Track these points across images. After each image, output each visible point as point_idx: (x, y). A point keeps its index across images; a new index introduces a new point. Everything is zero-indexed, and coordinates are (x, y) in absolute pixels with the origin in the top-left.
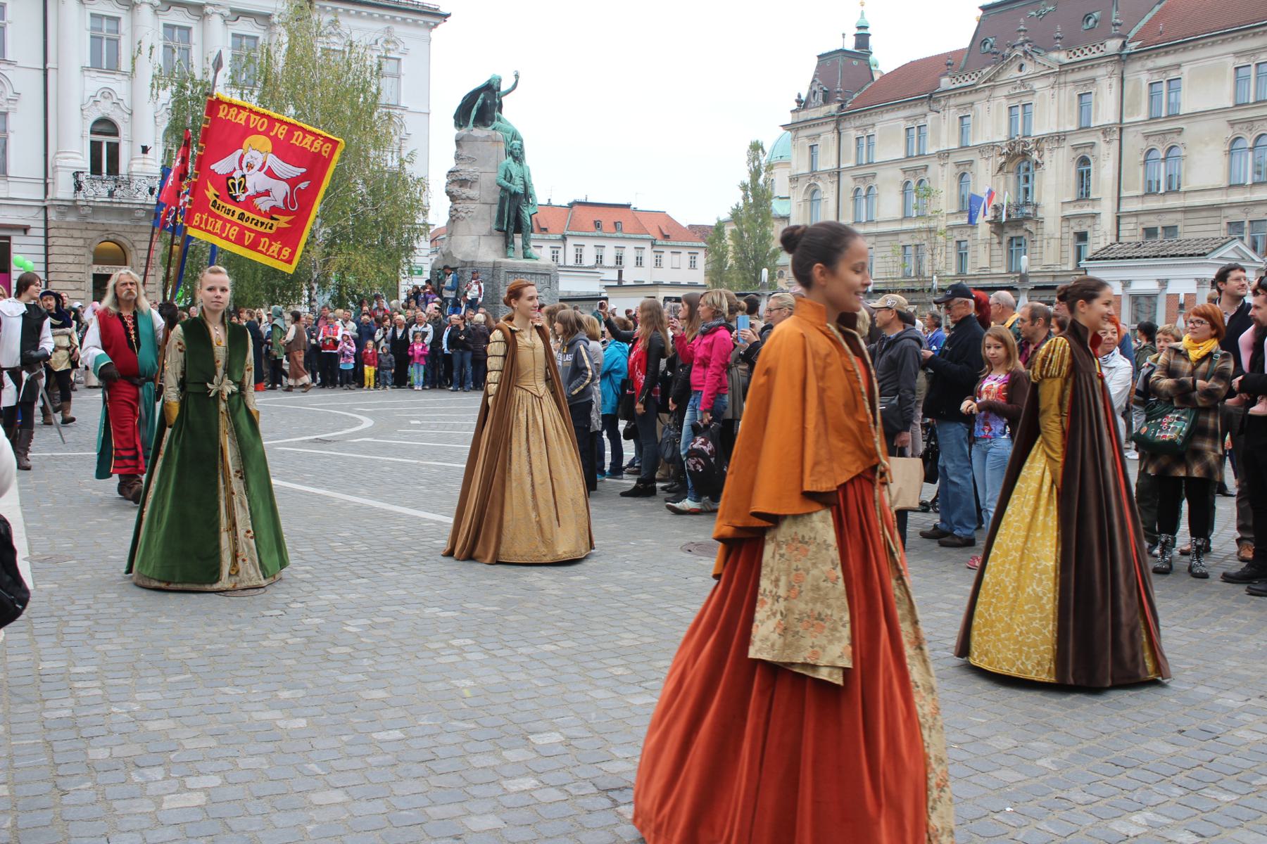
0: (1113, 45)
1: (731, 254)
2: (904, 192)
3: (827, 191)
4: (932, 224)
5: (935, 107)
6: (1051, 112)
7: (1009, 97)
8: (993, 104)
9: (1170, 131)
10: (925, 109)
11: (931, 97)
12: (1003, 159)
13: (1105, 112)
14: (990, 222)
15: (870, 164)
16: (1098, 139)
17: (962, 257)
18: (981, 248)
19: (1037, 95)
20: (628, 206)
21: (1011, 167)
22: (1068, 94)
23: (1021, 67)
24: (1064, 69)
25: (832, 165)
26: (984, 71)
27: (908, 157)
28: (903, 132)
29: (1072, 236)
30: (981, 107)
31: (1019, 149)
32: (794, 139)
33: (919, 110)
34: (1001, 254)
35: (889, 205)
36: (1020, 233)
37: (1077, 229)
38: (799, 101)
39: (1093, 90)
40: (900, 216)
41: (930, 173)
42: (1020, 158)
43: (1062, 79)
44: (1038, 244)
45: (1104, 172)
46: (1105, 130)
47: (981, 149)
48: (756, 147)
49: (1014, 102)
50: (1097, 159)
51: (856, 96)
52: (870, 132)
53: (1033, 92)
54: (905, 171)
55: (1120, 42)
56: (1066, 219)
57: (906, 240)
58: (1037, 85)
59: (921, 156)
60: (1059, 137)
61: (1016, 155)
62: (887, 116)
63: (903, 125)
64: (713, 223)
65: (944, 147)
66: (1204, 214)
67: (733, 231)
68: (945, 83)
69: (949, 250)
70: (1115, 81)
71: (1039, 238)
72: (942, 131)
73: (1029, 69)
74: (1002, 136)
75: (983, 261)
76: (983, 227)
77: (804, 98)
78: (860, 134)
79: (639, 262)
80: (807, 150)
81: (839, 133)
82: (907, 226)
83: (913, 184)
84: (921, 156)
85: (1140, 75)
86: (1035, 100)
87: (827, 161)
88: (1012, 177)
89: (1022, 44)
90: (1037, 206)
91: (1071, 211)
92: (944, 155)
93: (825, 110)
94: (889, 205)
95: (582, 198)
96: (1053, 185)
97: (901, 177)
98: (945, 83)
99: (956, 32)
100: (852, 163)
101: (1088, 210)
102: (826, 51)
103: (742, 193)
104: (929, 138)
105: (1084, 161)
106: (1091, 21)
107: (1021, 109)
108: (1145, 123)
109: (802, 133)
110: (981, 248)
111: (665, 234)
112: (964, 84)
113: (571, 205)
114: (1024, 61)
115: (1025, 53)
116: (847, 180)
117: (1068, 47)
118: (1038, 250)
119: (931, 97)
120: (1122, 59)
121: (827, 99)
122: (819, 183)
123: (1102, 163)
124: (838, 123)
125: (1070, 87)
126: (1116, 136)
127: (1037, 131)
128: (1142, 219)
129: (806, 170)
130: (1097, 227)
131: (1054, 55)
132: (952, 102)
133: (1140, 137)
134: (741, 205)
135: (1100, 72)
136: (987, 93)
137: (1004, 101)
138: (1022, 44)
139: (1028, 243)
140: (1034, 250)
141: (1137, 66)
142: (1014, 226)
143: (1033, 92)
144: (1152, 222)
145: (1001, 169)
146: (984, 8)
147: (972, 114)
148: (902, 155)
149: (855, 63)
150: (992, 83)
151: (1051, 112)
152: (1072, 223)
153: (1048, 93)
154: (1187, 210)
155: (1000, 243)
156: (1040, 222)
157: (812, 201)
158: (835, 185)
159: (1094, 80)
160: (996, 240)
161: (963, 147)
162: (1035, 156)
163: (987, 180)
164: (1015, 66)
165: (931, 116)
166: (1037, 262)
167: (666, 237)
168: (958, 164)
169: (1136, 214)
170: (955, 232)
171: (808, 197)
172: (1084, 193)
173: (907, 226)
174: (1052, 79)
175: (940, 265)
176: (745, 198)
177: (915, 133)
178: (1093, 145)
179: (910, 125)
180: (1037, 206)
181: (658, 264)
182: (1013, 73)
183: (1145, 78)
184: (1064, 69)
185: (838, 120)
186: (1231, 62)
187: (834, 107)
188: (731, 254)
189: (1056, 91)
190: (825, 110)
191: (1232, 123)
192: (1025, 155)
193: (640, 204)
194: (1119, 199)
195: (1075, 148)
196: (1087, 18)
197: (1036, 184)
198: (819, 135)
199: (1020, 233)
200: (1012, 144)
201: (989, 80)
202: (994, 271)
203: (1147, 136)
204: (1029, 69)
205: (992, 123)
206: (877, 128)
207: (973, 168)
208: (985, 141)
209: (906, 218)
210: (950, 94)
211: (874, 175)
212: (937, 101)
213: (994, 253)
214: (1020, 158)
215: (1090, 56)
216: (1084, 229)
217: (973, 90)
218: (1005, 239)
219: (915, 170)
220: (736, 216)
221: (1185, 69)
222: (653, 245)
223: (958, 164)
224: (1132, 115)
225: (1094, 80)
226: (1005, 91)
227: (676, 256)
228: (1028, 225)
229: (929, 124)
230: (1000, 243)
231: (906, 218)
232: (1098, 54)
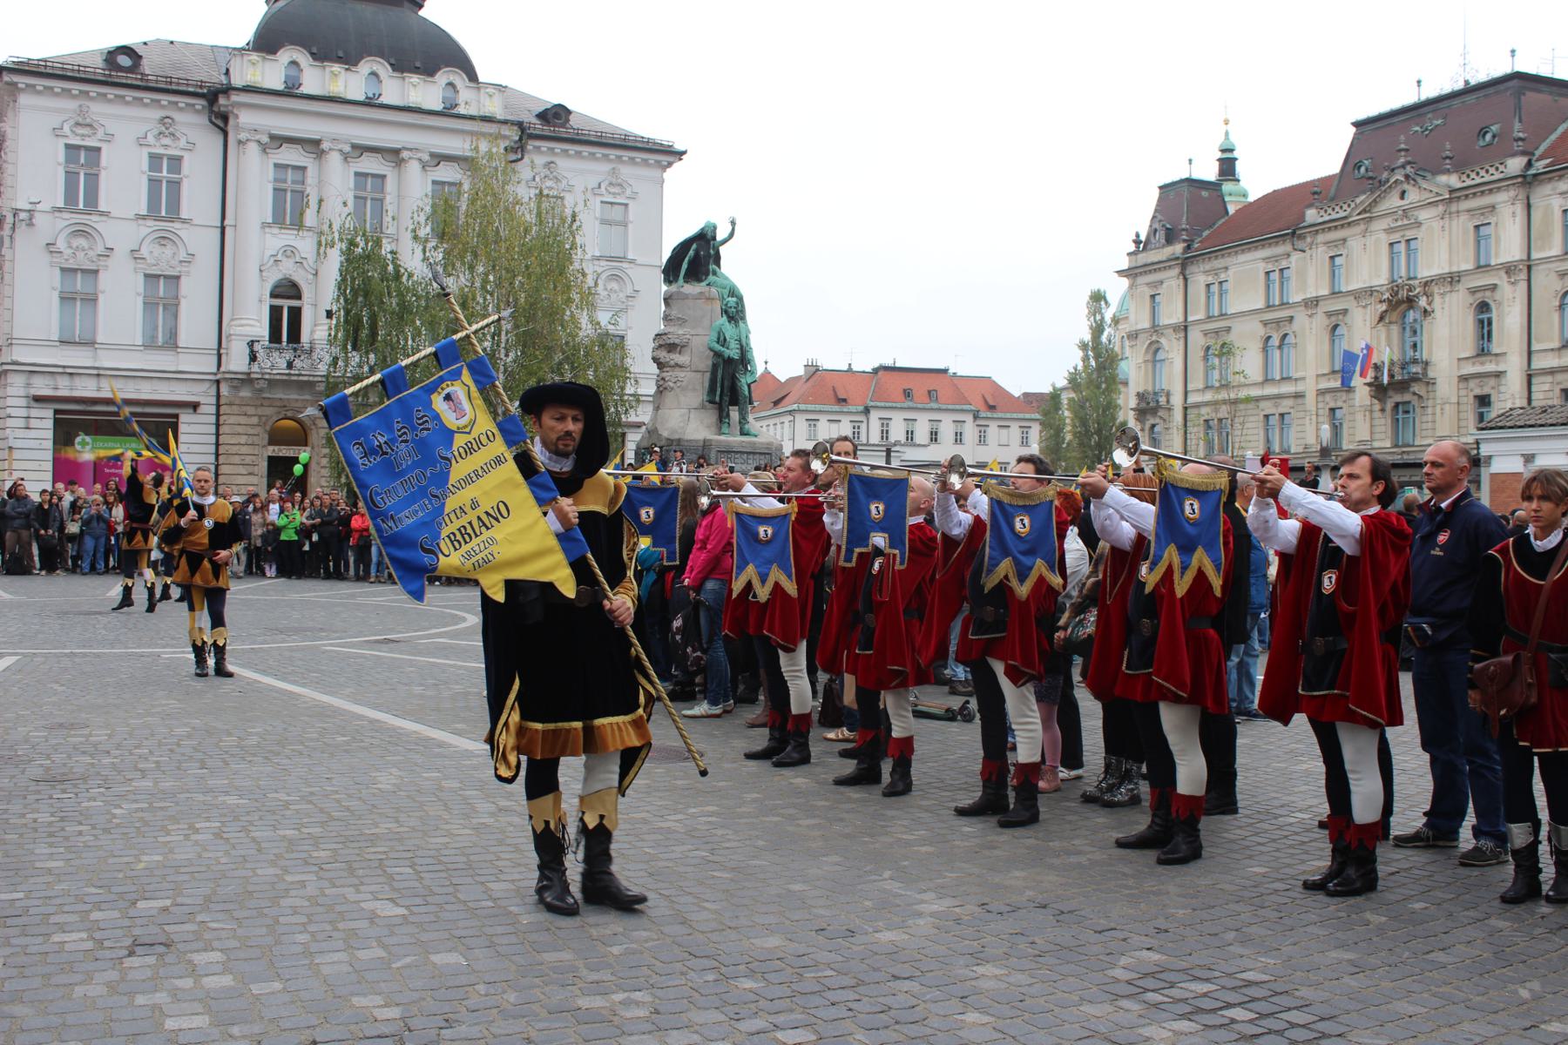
0: (1515, 165)
1: (1068, 428)
2: (1265, 350)
3: (1172, 350)
4: (1300, 387)
5: (1300, 244)
6: (1441, 248)
7: (1389, 231)
8: (1370, 240)
10: (1287, 247)
12: (1384, 307)
13: (1509, 246)
14: (1369, 384)
16: (1501, 279)
17: (1336, 429)
18: (1359, 416)
19: (1423, 228)
20: (945, 371)
21: (1395, 316)
23: (1403, 195)
24: (1455, 195)
25: (1177, 318)
26: (1358, 200)
28: (1262, 276)
29: (1471, 400)
30: (1355, 244)
31: (1403, 294)
32: (1131, 287)
34: (1384, 423)
35: (1249, 363)
36: (1407, 397)
37: (1478, 392)
38: (1137, 242)
40: (1260, 379)
41: (1296, 325)
42: (1402, 303)
43: (1454, 207)
44: (1430, 411)
45: (1509, 320)
46: (1509, 269)
47: (1357, 295)
48: (1098, 298)
49: (1395, 237)
50: (1500, 304)
51: (1205, 234)
52: (1223, 277)
53: (1419, 224)
54: (1265, 324)
55: (1524, 160)
56: (1464, 379)
57: (1268, 408)
58: (1423, 215)
60: (1453, 279)
61: (1400, 302)
62: (1242, 258)
63: (1262, 267)
64: (1047, 389)
65: (1311, 293)
67: (1071, 400)
68: (1311, 215)
69: (1321, 419)
70: (1519, 208)
71: (1430, 403)
72: (1308, 273)
73: (1413, 196)
74: (1381, 279)
75: (1362, 432)
77: (1143, 238)
78: (1210, 279)
79: (959, 438)
80: (1148, 299)
81: (1186, 280)
83: (1275, 341)
86: (1420, 233)
87: (1171, 314)
88: (1395, 329)
89: (1403, 167)
92: (1312, 303)
93: (1168, 251)
94: (1249, 363)
95: (889, 363)
96: (1446, 339)
97: (1261, 331)
99: (1324, 158)
100: (1201, 316)
101: (1490, 367)
102: (1168, 181)
103: (1081, 354)
104: (1293, 284)
105: (1483, 307)
106: (1488, 137)
107: (1404, 245)
108: (1559, 259)
109: (1141, 280)
110: (1359, 416)
111: (989, 402)
112: (1334, 216)
113: (876, 371)
114: (1406, 186)
115: (1407, 177)
116: (1196, 336)
117: (1460, 167)
118: (1430, 418)
119: (1294, 233)
120: (1527, 181)
121: (1170, 238)
122: (1163, 340)
123: (1507, 309)
124: (1184, 266)
125: (1464, 217)
126: (1524, 276)
127: (1425, 272)
128: (1559, 377)
129: (1146, 324)
130: (1502, 389)
131: (1443, 179)
132: (1321, 238)
133: (1554, 276)
134: (1080, 367)
135: (1501, 198)
136: (1362, 226)
137: (1383, 236)
138: (1403, 167)
139: (1418, 410)
140: (1425, 419)
141: (1547, 189)
142: (1399, 388)
143: (1419, 224)
145: (1381, 318)
146: (1357, 124)
147: (1344, 252)
148: (1260, 304)
149: (1205, 194)
150: (1368, 215)
151: (1441, 248)
152: (1472, 384)
153: (1436, 225)
155: (1383, 410)
156: (1430, 383)
157: (1154, 362)
158: (1182, 342)
159: (1493, 207)
160: (1377, 407)
161: (1335, 294)
162: (1423, 302)
163: (1364, 332)
165: (1295, 256)
166: (1430, 433)
167: (992, 408)
168: (1329, 314)
169: (1552, 372)
170: (1328, 397)
171: (1149, 357)
173: (1270, 390)
174: (1441, 208)
176: (1085, 359)
177: (1276, 277)
178: (1494, 287)
179: (1270, 267)
181: (982, 440)
182: (1393, 202)
184: (1455, 195)
187: (1178, 248)
188: (1068, 428)
189: (1447, 221)
192: (1410, 302)
193: (962, 367)
194: (1530, 353)
195: (1473, 291)
196: (1483, 132)
197: (1425, 338)
199: (1407, 397)
200: (1395, 289)
201: (1364, 211)
202: (1376, 444)
204: (1413, 196)
205: (1368, 263)
206: (1230, 272)
207: (1348, 319)
208: (1361, 285)
209: (1267, 380)
210: (1318, 228)
211: (1228, 329)
213: (1376, 422)
214: (1402, 303)
215: (1487, 178)
218: (1389, 405)
219: (1278, 322)
220: (1073, 381)
222: (976, 417)
223: (1329, 314)
224: (1542, 249)
225: (1493, 207)
227: (1004, 431)
228: (1416, 388)
229: (1293, 265)
230: (1383, 410)
231: (1267, 380)
232: (1497, 176)
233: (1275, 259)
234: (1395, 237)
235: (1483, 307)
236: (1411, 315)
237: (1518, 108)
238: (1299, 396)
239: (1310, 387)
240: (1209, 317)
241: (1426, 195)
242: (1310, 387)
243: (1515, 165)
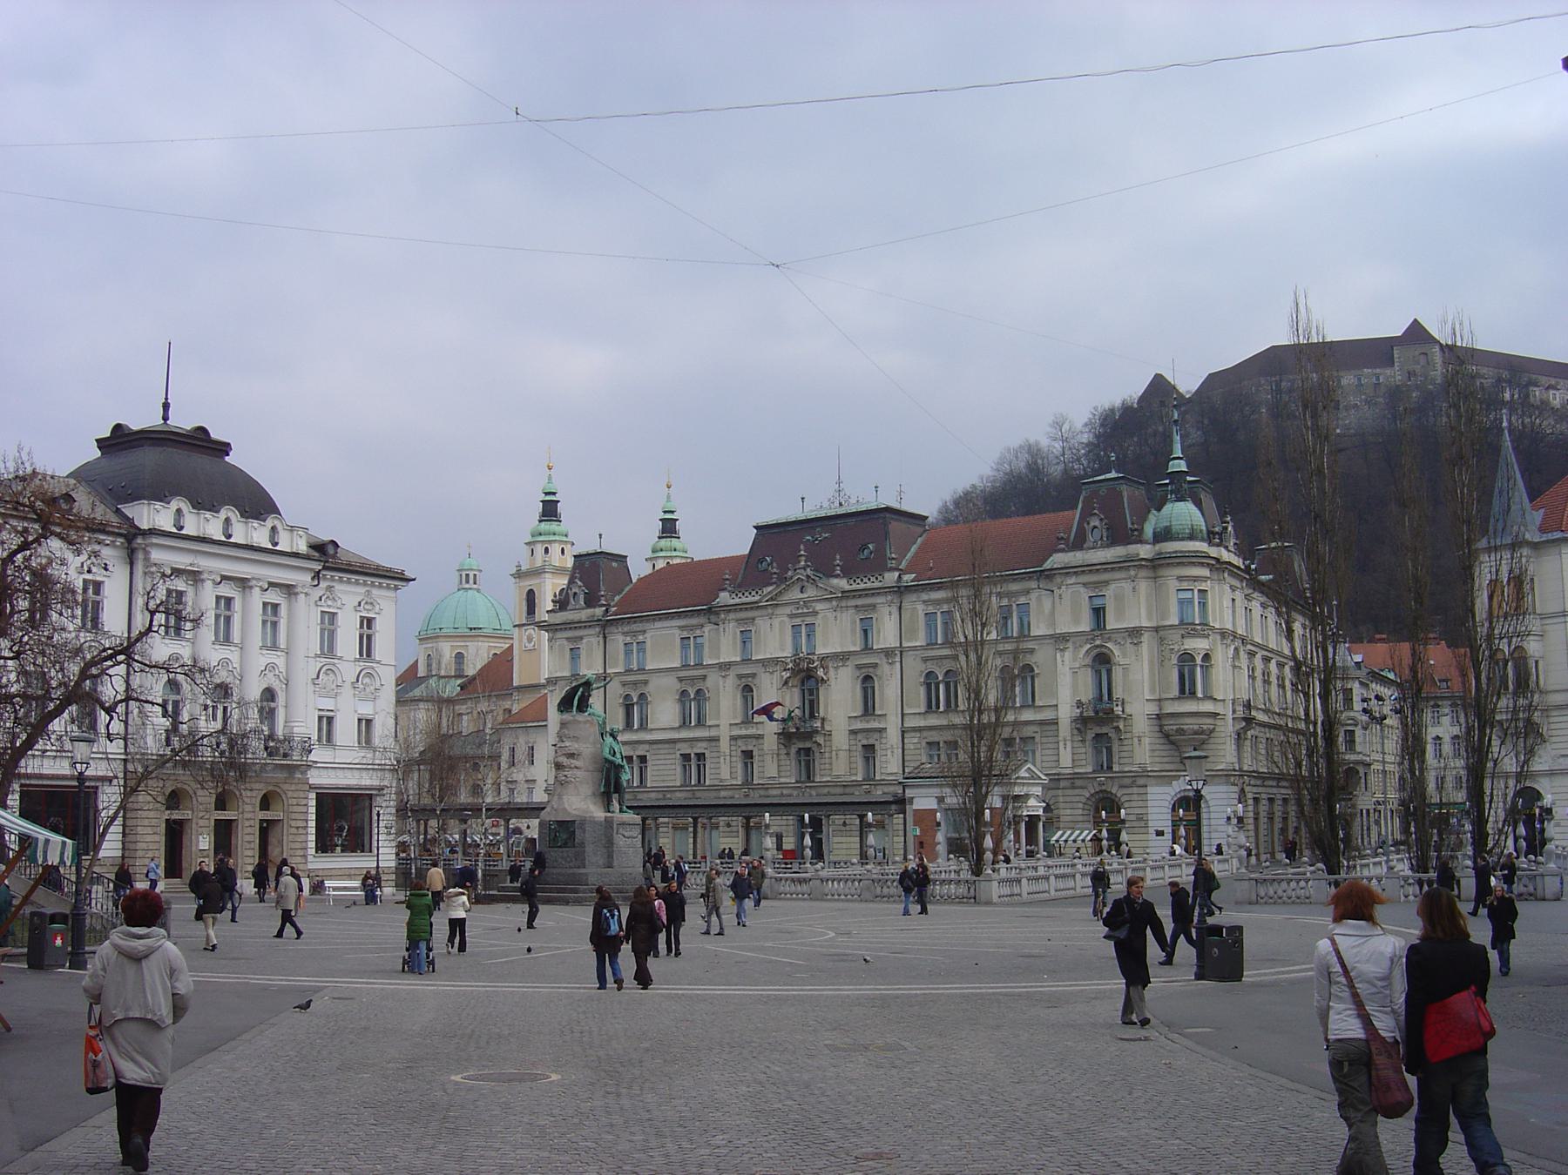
0: (891, 578)
4: (713, 733)
5: (713, 618)
6: (835, 633)
7: (791, 616)
8: (776, 622)
10: (702, 620)
11: (712, 612)
12: (786, 675)
13: (887, 633)
15: (642, 670)
18: (768, 758)
24: (846, 595)
27: (685, 666)
28: (678, 641)
33: (694, 621)
35: (664, 713)
36: (808, 745)
37: (865, 742)
39: (874, 616)
41: (709, 683)
45: (888, 692)
46: (888, 653)
49: (797, 621)
50: (880, 678)
51: (617, 598)
52: (641, 638)
53: (815, 613)
54: (680, 680)
56: (853, 732)
58: (819, 607)
59: (699, 665)
60: (843, 657)
61: (801, 671)
62: (658, 624)
72: (723, 644)
74: (788, 652)
75: (771, 770)
76: (771, 743)
82: (684, 734)
84: (699, 665)
86: (818, 621)
88: (796, 691)
90: (823, 720)
91: (859, 725)
92: (725, 667)
94: (664, 713)
96: (839, 700)
98: (724, 598)
101: (875, 725)
104: (706, 650)
105: (868, 678)
107: (804, 628)
109: (559, 635)
110: (768, 758)
112: (744, 600)
117: (847, 573)
120: (900, 591)
121: (591, 601)
124: (604, 627)
125: (852, 611)
127: (821, 650)
128: (925, 734)
131: (835, 581)
132: (732, 616)
135: (879, 600)
137: (786, 619)
141: (913, 597)
142: (802, 738)
143: (815, 613)
144: (934, 736)
145: (786, 683)
150: (774, 603)
151: (835, 633)
152: (859, 736)
153: (830, 615)
159: (874, 606)
161: (746, 661)
164: (797, 588)
169: (919, 729)
170: (740, 742)
172: (868, 708)
173: (684, 734)
175: (725, 773)
178: (875, 666)
180: (823, 720)
182: (795, 594)
185: (605, 626)
187: (599, 611)
190: (584, 615)
195: (859, 667)
196: (864, 547)
198: (581, 638)
200: (797, 660)
203: (925, 660)
204: (811, 592)
207: (756, 681)
211: (646, 682)
212: (717, 613)
214: (806, 677)
215: (869, 585)
216: (871, 742)
217: (754, 606)
218: (793, 750)
225: (874, 606)
226: (788, 610)
231: (684, 724)
232: (877, 584)
233: (691, 628)
234: (797, 621)
235: (868, 678)
236: (812, 683)
237: (886, 533)
238: (715, 739)
239: (724, 733)
240: (628, 671)
242: (724, 733)
243: (891, 578)
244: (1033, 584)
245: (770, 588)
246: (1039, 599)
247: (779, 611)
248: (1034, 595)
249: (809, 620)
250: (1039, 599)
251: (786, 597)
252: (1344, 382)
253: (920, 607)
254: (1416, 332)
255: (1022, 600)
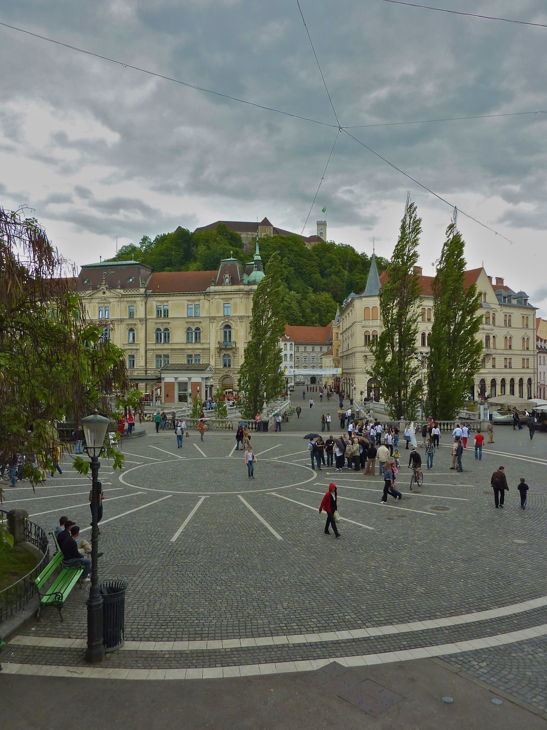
9: (165, 323)
13: (140, 313)
22: (124, 305)
24: (123, 296)
43: (122, 299)
46: (141, 320)
50: (137, 329)
58: (111, 300)
60: (121, 321)
61: (102, 325)
66: (178, 351)
70: (144, 303)
85: (154, 302)
101: (135, 347)
115: (107, 288)
117: (122, 287)
120: (146, 296)
123: (139, 331)
127: (111, 317)
128: (155, 351)
130: (138, 354)
137: (97, 304)
141: (152, 299)
144: (159, 353)
153: (116, 304)
154: (172, 349)
162: (111, 326)
169: (153, 350)
182: (100, 294)
183: (155, 303)
184: (123, 296)
186: (186, 302)
191: (187, 323)
195: (128, 325)
203: (156, 323)
204: (108, 294)
215: (133, 293)
221: (170, 303)
224: (150, 316)
226: (97, 301)
232: (136, 293)
234: (101, 305)
237: (139, 272)
241: (112, 295)
244: (202, 297)
245: (89, 292)
246: (203, 303)
247: (93, 301)
248: (201, 302)
249: (106, 305)
250: (203, 303)
251: (96, 296)
252: (242, 236)
253: (155, 303)
254: (266, 222)
255: (197, 303)
